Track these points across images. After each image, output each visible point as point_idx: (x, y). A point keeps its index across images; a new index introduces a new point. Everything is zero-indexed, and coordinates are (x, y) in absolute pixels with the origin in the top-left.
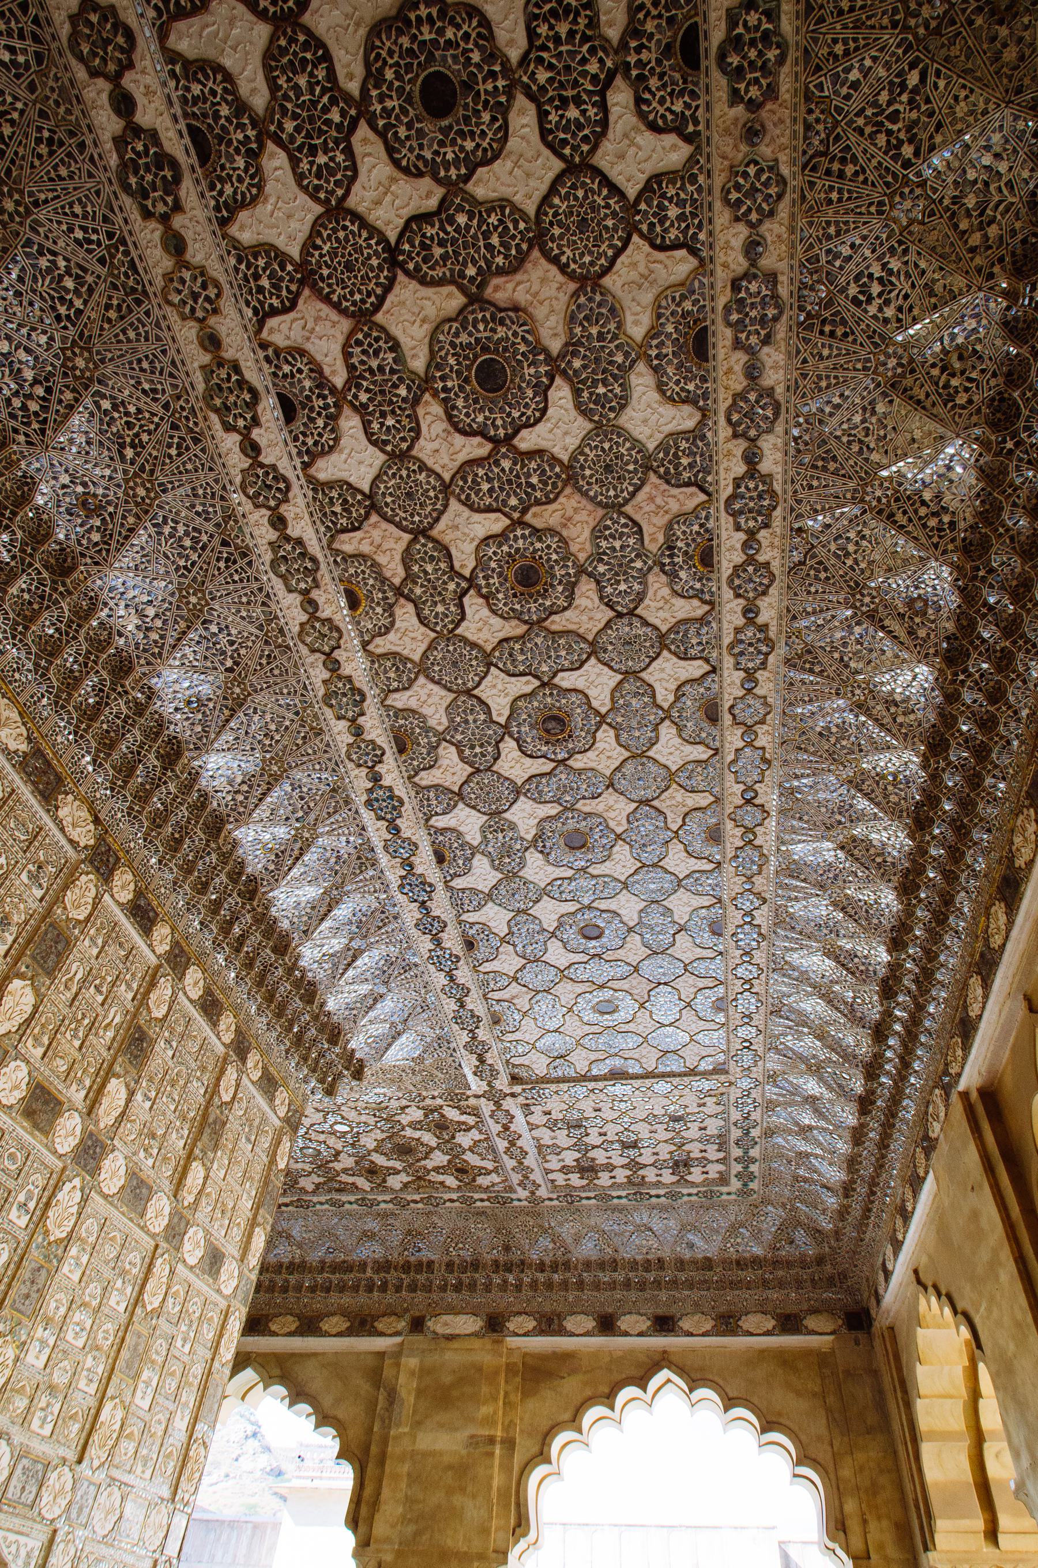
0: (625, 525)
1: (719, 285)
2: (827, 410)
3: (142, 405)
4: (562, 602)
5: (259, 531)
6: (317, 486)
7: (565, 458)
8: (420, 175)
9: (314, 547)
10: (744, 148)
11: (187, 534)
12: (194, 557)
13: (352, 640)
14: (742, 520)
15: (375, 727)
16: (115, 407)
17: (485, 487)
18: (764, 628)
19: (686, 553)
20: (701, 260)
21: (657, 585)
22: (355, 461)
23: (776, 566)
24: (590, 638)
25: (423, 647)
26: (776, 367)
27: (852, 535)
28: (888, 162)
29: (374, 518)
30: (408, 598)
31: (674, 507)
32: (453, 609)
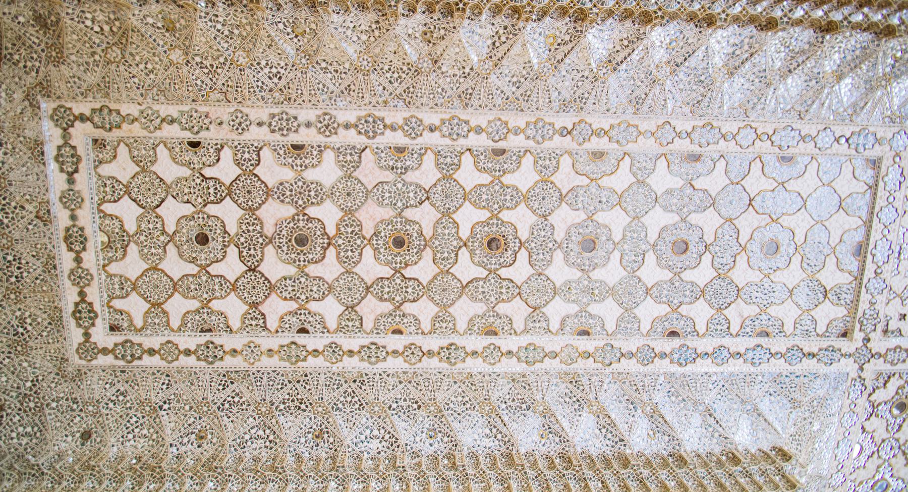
0: (378, 190)
1: (273, 139)
2: (326, 90)
3: (287, 392)
4: (416, 227)
5: (352, 364)
6: (340, 329)
7: (342, 214)
8: (225, 252)
9: (366, 341)
10: (224, 126)
11: (345, 397)
12: (356, 399)
13: (419, 340)
14: (379, 131)
15: (477, 342)
16: (284, 403)
17: (349, 253)
18: (443, 122)
19: (396, 161)
20: (265, 145)
21: (413, 177)
22: (330, 309)
23: (407, 115)
24: (440, 216)
25: (431, 304)
26: (307, 114)
27: (388, 75)
28: (226, 68)
29: (357, 308)
30: (401, 304)
31: (372, 165)
32: (411, 283)
